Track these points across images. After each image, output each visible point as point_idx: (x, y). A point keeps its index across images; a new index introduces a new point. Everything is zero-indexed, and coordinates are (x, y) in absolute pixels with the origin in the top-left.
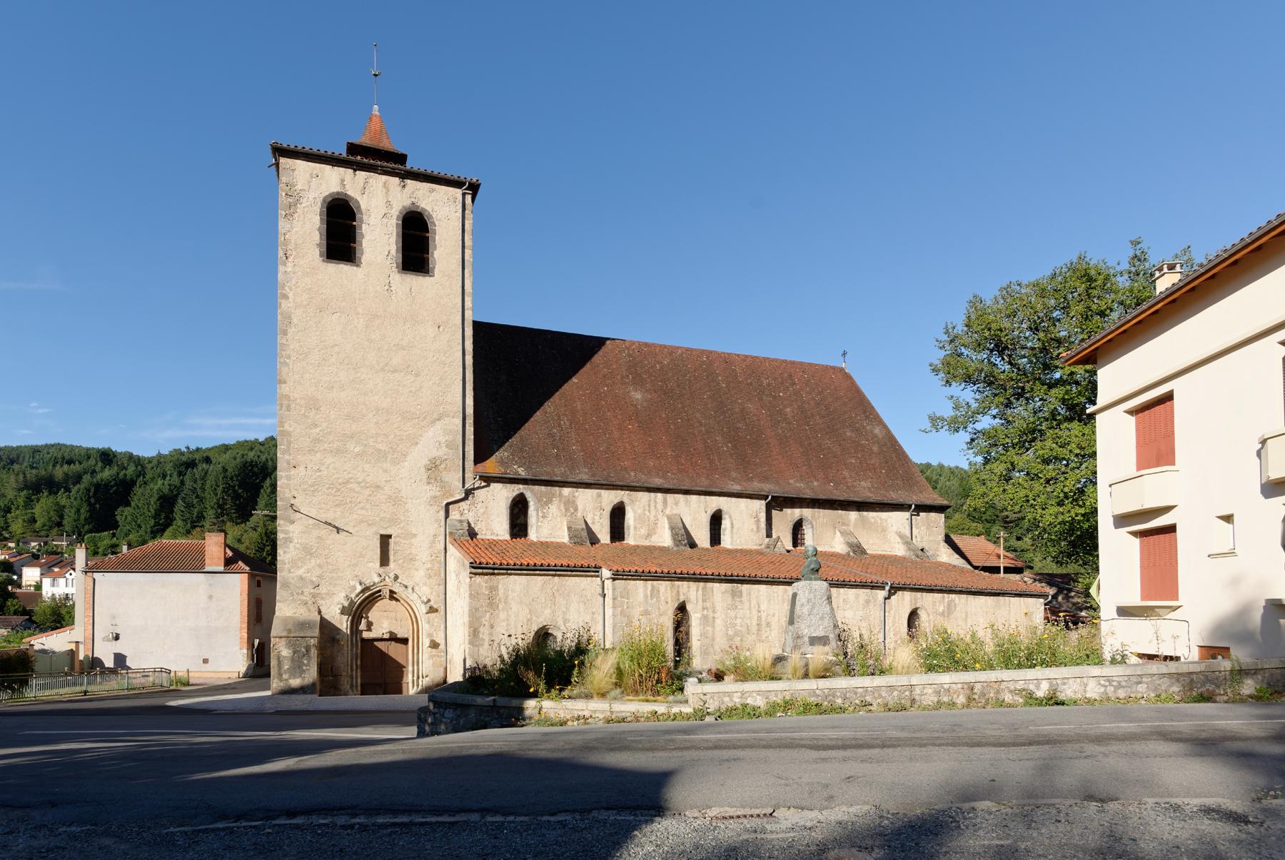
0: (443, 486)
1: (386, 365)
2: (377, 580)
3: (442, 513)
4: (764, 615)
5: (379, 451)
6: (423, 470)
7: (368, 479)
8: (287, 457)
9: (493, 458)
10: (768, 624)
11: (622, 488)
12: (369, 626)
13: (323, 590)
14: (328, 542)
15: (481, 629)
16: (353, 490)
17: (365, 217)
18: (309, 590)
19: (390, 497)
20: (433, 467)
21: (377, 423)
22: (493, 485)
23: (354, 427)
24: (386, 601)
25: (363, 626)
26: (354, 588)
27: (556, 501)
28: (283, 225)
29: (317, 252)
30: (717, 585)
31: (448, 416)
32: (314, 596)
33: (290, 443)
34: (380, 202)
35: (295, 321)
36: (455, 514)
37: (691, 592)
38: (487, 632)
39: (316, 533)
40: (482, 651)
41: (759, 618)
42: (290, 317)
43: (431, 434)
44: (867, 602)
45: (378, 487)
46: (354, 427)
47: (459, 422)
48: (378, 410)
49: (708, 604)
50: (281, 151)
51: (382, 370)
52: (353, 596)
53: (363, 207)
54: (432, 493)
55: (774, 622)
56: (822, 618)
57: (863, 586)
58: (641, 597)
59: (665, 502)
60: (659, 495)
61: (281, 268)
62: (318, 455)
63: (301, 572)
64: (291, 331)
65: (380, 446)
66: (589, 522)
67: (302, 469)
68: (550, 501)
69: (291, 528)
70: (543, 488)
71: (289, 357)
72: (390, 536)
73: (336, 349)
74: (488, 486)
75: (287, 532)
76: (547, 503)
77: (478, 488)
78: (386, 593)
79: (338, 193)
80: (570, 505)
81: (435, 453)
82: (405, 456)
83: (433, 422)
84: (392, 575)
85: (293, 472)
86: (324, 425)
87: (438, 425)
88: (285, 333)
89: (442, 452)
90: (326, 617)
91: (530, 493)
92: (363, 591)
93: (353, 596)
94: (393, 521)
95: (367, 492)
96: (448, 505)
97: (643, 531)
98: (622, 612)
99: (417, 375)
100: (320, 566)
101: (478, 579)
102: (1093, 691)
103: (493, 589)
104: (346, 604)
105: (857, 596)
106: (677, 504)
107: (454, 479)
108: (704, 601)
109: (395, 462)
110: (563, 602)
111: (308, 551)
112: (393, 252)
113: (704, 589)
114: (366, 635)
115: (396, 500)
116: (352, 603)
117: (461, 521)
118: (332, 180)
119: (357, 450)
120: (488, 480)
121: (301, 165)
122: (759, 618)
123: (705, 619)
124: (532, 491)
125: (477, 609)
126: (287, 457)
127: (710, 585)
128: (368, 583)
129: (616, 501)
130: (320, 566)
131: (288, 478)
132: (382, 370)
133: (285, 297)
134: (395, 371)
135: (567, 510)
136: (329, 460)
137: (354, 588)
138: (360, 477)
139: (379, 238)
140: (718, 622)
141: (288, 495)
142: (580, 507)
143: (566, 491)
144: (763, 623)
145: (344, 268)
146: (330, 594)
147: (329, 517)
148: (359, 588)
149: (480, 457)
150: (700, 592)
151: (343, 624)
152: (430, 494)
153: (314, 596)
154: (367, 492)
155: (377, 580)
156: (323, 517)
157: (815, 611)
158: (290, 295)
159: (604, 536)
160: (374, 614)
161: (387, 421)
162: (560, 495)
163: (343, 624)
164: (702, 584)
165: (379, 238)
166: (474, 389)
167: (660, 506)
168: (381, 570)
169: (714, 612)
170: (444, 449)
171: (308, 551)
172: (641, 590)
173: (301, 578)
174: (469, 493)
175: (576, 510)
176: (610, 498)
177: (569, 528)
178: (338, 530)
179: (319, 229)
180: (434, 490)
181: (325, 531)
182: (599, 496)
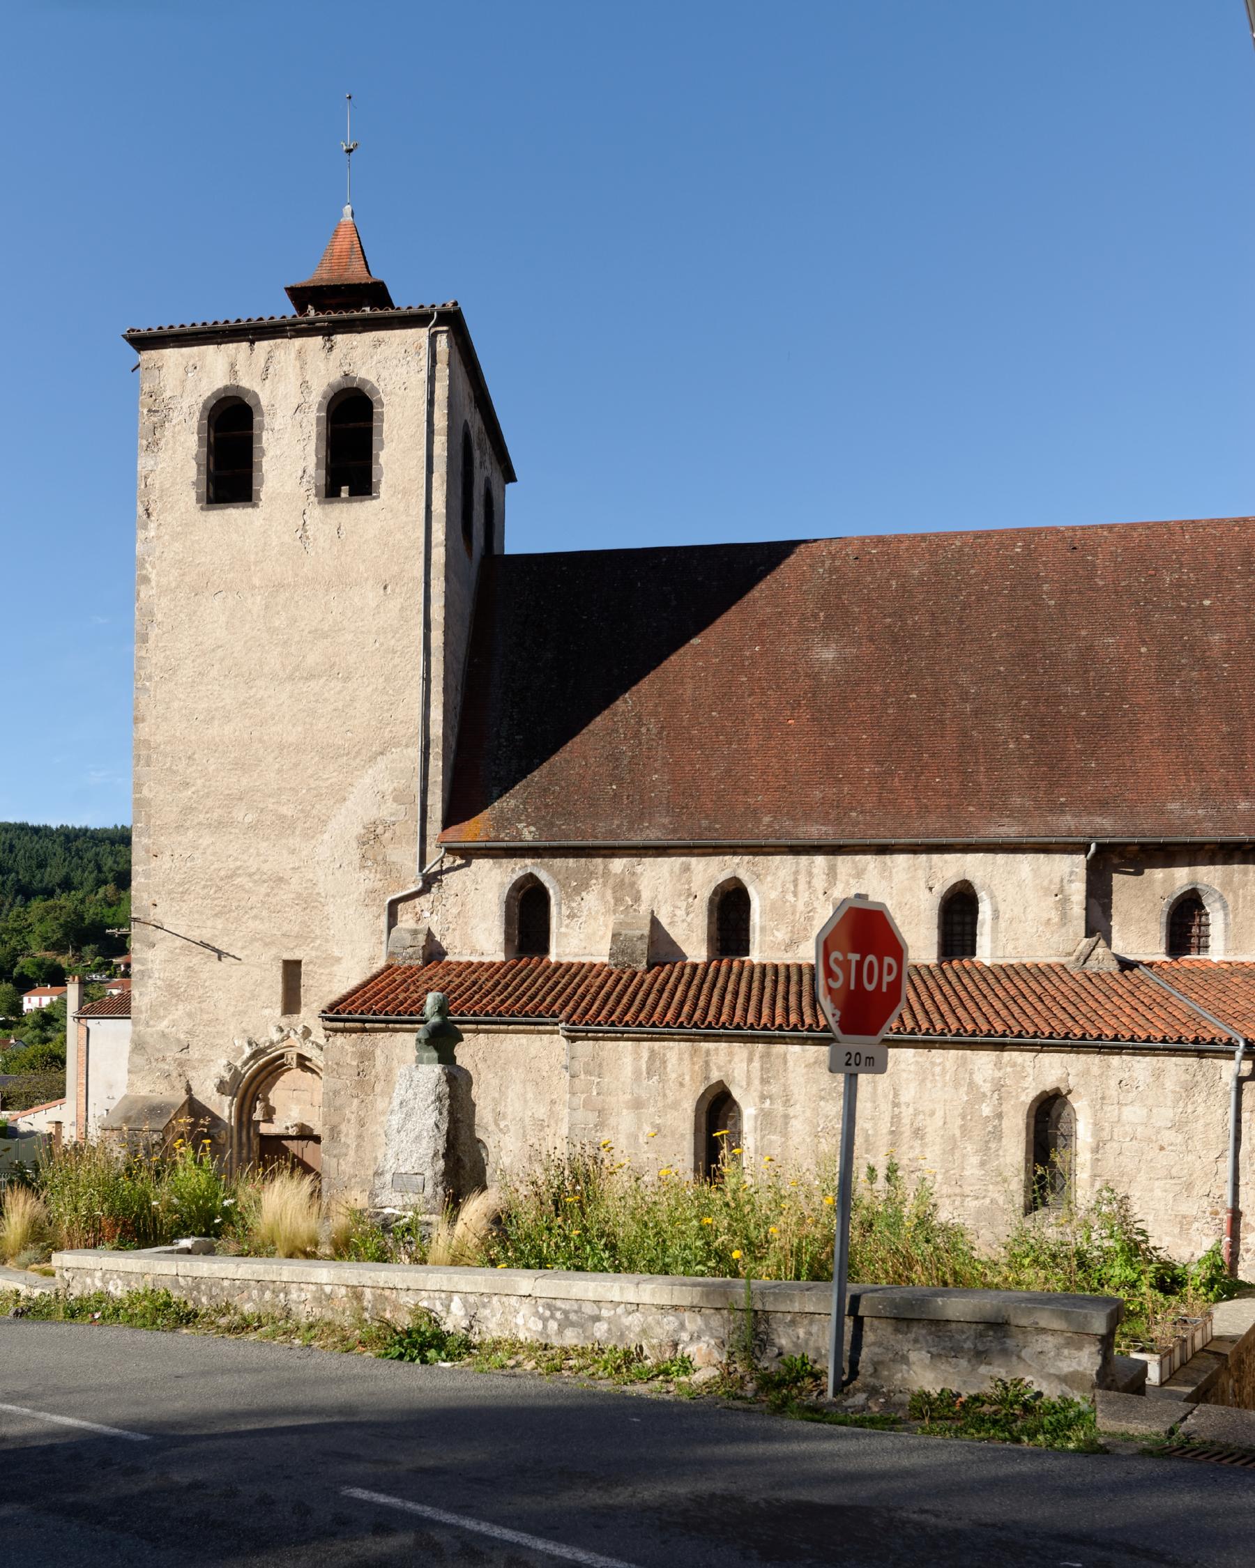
0: (389, 870)
1: (297, 668)
2: (276, 1036)
3: (384, 919)
4: (907, 1113)
5: (282, 818)
6: (355, 845)
7: (265, 867)
8: (145, 841)
9: (486, 814)
10: (918, 1133)
11: (734, 850)
12: (269, 1114)
13: (194, 1054)
14: (204, 976)
15: (343, 1128)
16: (242, 887)
17: (267, 420)
18: (172, 1054)
19: (299, 895)
20: (372, 837)
21: (279, 771)
22: (478, 863)
23: (244, 781)
24: (297, 1072)
25: (258, 1115)
26: (240, 1051)
27: (596, 885)
28: (144, 463)
29: (193, 495)
30: (796, 1049)
31: (398, 745)
32: (181, 1064)
33: (149, 816)
34: (290, 384)
35: (159, 617)
36: (406, 920)
37: (735, 1064)
38: (353, 1133)
39: (185, 961)
40: (343, 1167)
41: (896, 1119)
42: (152, 613)
43: (367, 780)
44: (1189, 1089)
45: (281, 879)
46: (244, 781)
47: (415, 753)
48: (281, 747)
49: (774, 1089)
50: (143, 342)
51: (291, 678)
52: (238, 1064)
53: (264, 402)
54: (369, 885)
55: (933, 1127)
56: (418, 1138)
57: (1176, 1048)
58: (628, 1071)
59: (832, 873)
60: (820, 861)
61: (141, 535)
62: (190, 833)
63: (163, 1025)
64: (154, 632)
65: (284, 810)
66: (664, 921)
67: (166, 857)
68: (584, 886)
69: (150, 954)
70: (571, 862)
71: (150, 678)
72: (298, 963)
73: (220, 653)
74: (468, 864)
75: (143, 962)
76: (577, 890)
77: (449, 870)
78: (292, 1059)
79: (226, 388)
80: (626, 890)
81: (374, 814)
82: (324, 823)
83: (373, 759)
84: (300, 1030)
85: (154, 863)
86: (199, 782)
87: (382, 762)
88: (144, 639)
89: (388, 810)
90: (199, 1098)
91: (545, 872)
92: (255, 1056)
93: (238, 1064)
94: (303, 938)
95: (263, 889)
96: (393, 904)
97: (781, 935)
98: (586, 1104)
99: (347, 679)
100: (190, 1015)
101: (340, 1039)
102: (526, 1326)
103: (365, 1057)
104: (227, 1077)
105: (1158, 1075)
106: (859, 874)
107: (406, 857)
108: (764, 1081)
109: (307, 836)
110: (495, 1082)
111: (173, 992)
112: (311, 470)
113: (766, 1056)
114: (265, 1129)
115: (309, 901)
116: (236, 1075)
117: (415, 932)
118: (216, 368)
119: (249, 819)
120: (468, 854)
121: (171, 355)
122: (896, 1119)
123: (766, 1118)
124: (549, 869)
125: (336, 1093)
126: (145, 841)
127: (779, 1049)
128: (263, 1042)
129: (722, 878)
130: (190, 1015)
131: (147, 875)
132: (291, 678)
133: (146, 580)
134: (311, 676)
135: (618, 901)
136: (206, 841)
137: (240, 1051)
138: (253, 865)
139: (289, 449)
140: (797, 1125)
141: (147, 902)
142: (646, 895)
143: (618, 865)
144: (907, 1131)
145: (235, 514)
146: (205, 1061)
147: (205, 935)
148: (248, 1051)
149: (459, 808)
150: (756, 1064)
151: (224, 1108)
152: (363, 887)
153: (181, 1064)
154: (263, 889)
155: (276, 1036)
156: (196, 935)
157: (409, 1126)
158: (153, 576)
159: (696, 950)
160: (277, 1095)
161: (296, 765)
162: (606, 873)
163: (224, 1108)
164: (760, 1047)
165: (289, 449)
166: (445, 690)
167: (820, 882)
168: (283, 1021)
169: (787, 1102)
170: (390, 806)
171: (173, 992)
172: (628, 1060)
173: (164, 1035)
174: (430, 881)
175: (637, 899)
176: (709, 872)
177: (615, 936)
178: (220, 954)
179: (197, 457)
180: (368, 880)
181: (198, 958)
182: (687, 869)
